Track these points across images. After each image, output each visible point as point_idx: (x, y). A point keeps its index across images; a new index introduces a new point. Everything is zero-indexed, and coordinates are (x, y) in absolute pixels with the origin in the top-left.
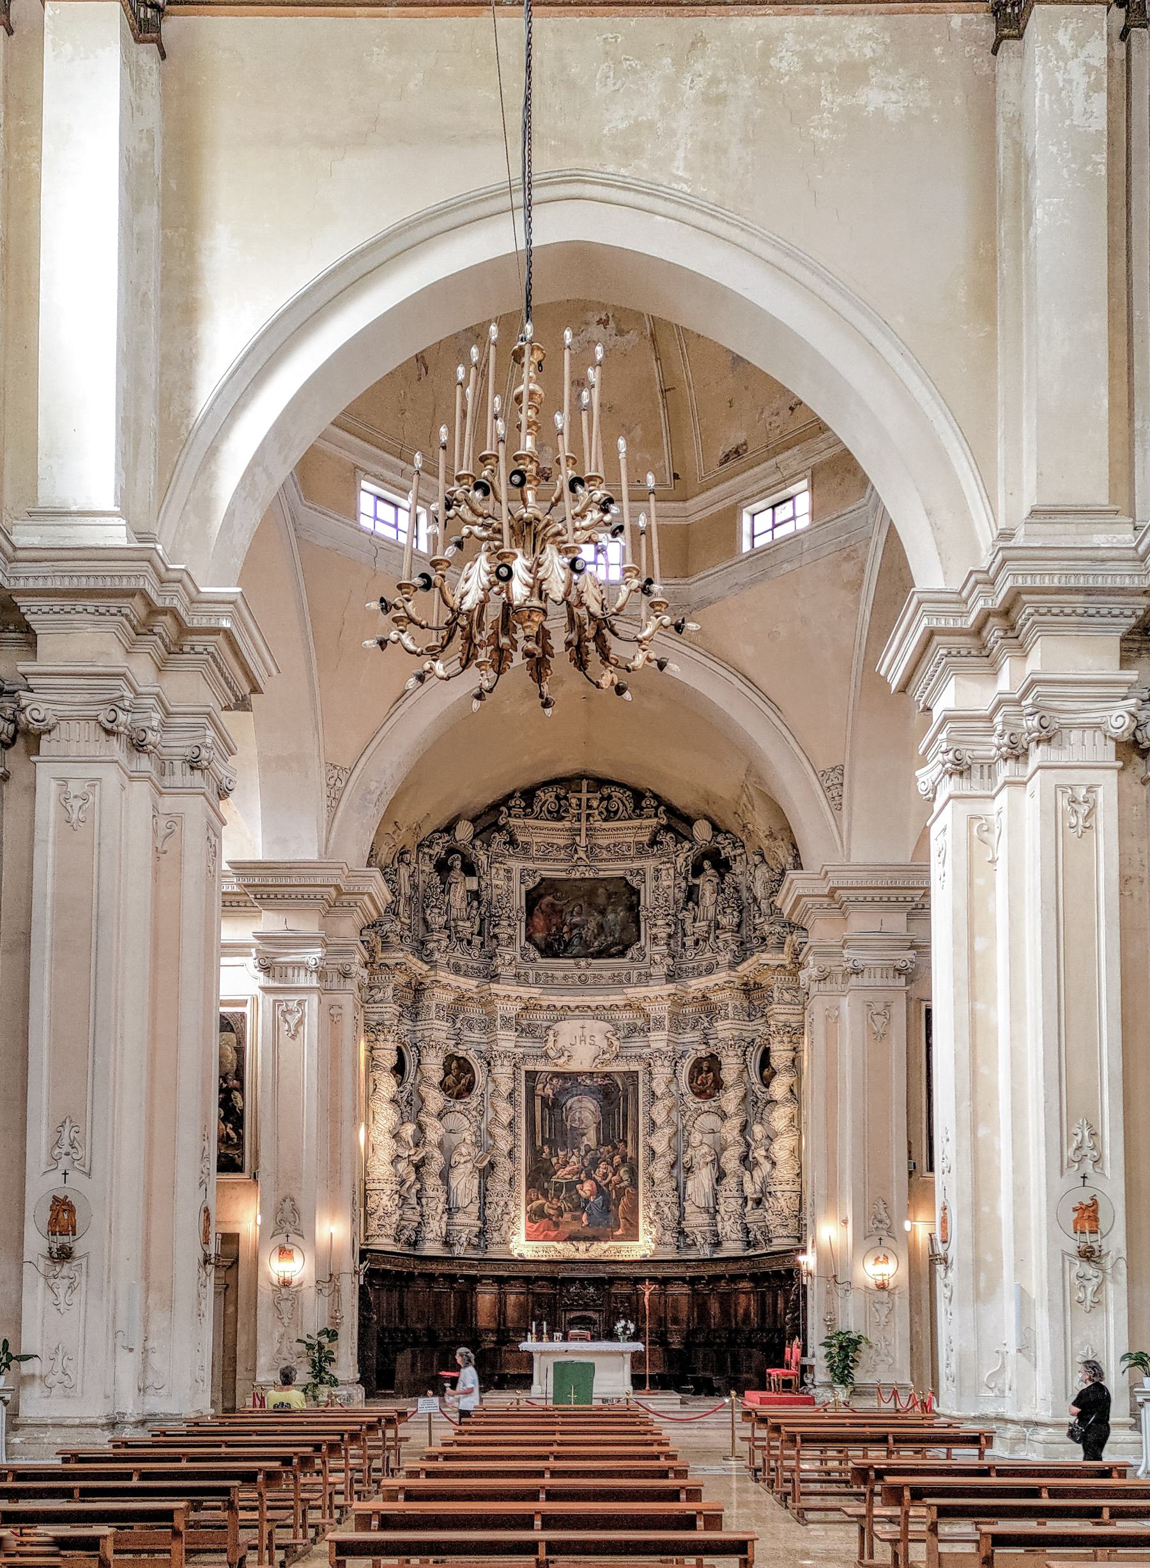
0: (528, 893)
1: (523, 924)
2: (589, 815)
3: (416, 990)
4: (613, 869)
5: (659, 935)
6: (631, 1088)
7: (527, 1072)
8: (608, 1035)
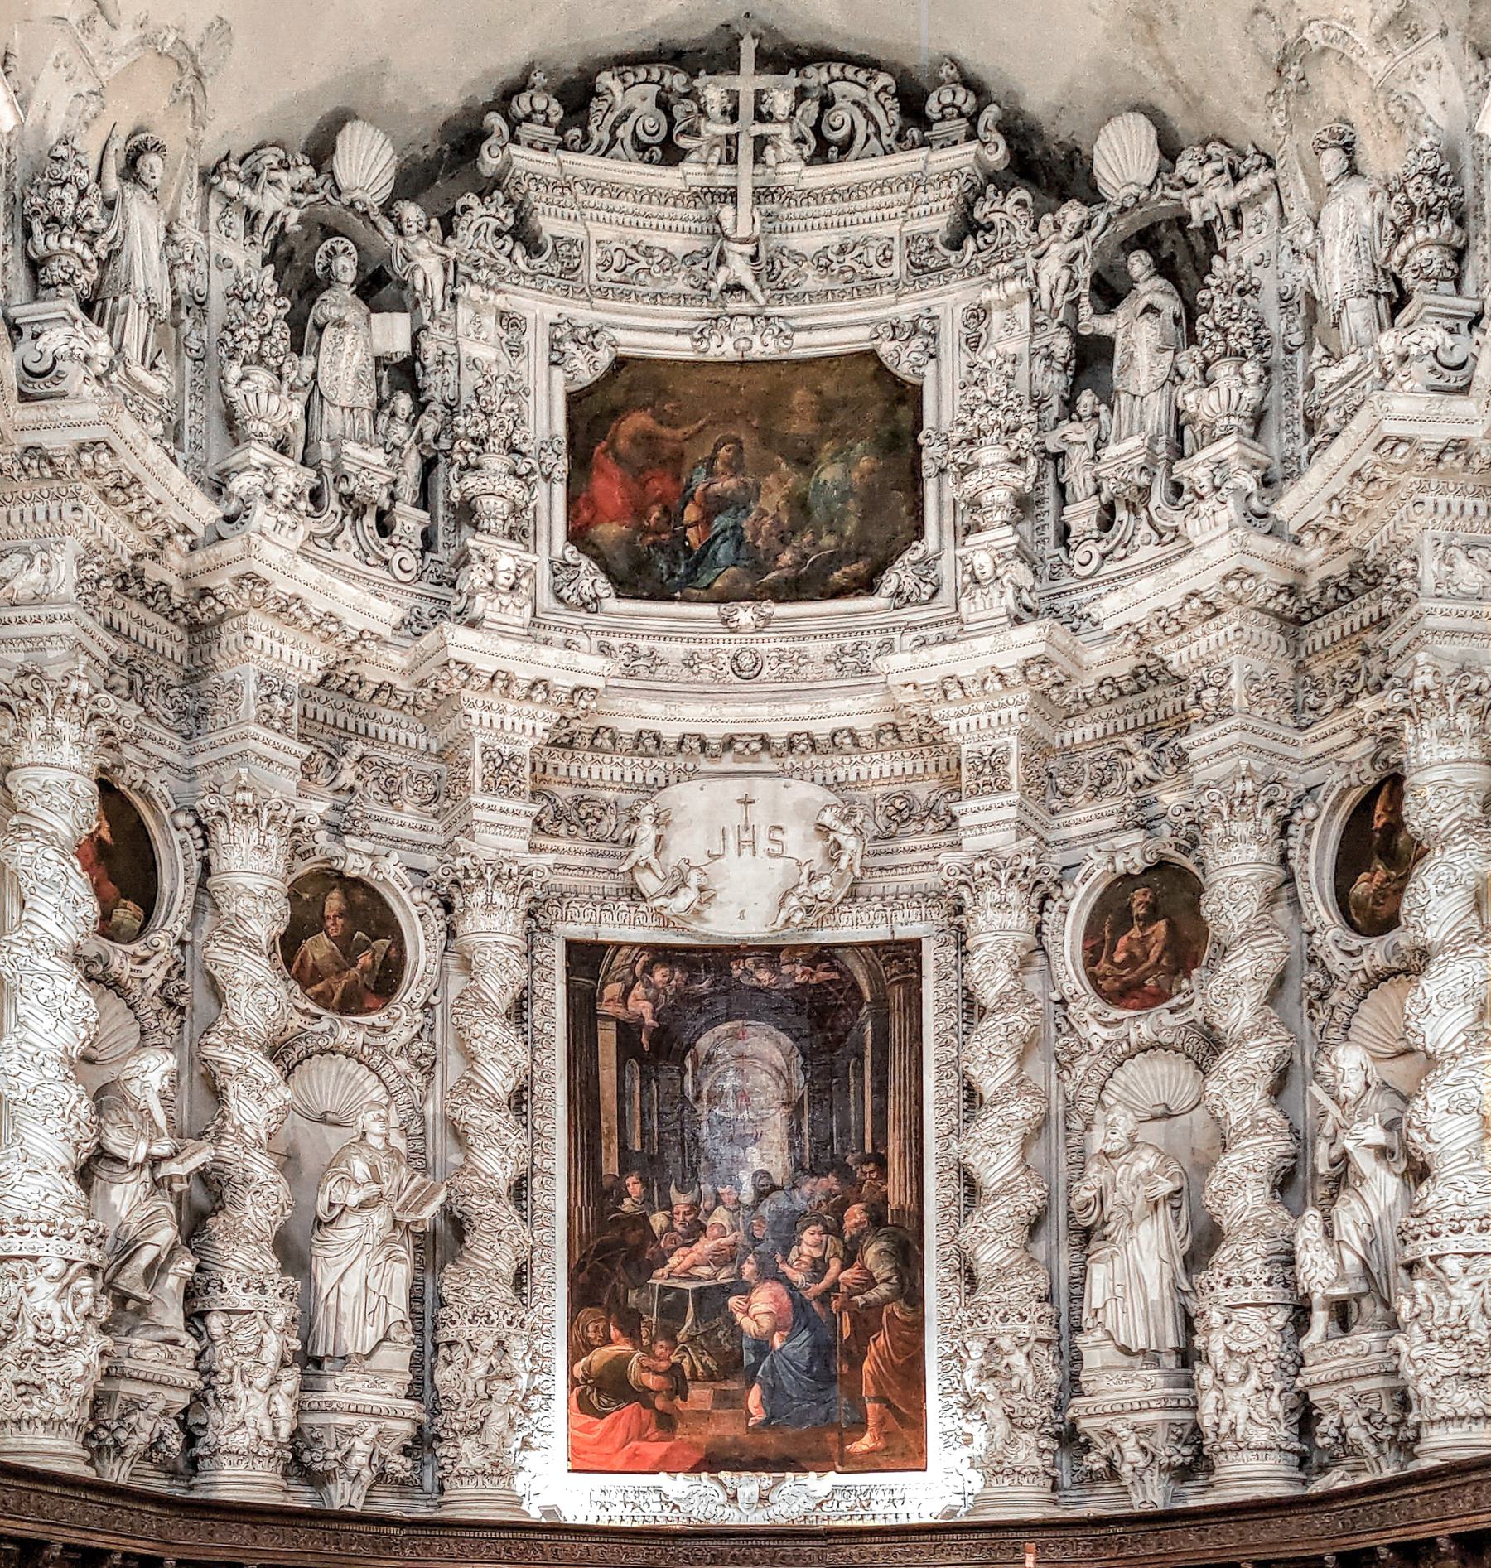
0: (574, 400)
1: (560, 490)
2: (761, 142)
3: (194, 627)
4: (832, 328)
5: (987, 498)
6: (897, 994)
7: (571, 945)
8: (828, 818)
